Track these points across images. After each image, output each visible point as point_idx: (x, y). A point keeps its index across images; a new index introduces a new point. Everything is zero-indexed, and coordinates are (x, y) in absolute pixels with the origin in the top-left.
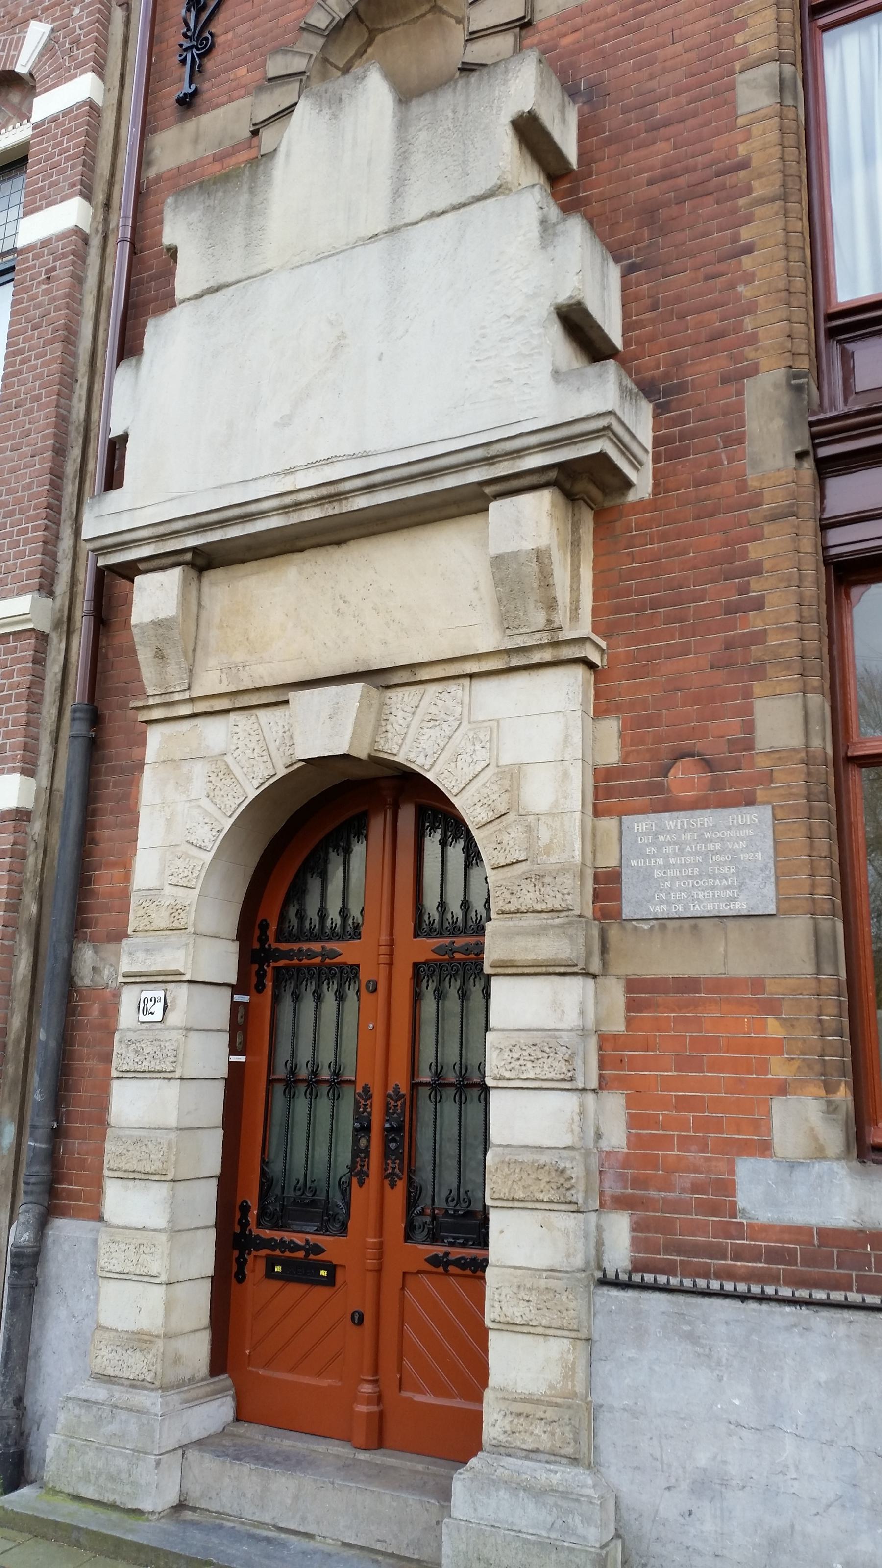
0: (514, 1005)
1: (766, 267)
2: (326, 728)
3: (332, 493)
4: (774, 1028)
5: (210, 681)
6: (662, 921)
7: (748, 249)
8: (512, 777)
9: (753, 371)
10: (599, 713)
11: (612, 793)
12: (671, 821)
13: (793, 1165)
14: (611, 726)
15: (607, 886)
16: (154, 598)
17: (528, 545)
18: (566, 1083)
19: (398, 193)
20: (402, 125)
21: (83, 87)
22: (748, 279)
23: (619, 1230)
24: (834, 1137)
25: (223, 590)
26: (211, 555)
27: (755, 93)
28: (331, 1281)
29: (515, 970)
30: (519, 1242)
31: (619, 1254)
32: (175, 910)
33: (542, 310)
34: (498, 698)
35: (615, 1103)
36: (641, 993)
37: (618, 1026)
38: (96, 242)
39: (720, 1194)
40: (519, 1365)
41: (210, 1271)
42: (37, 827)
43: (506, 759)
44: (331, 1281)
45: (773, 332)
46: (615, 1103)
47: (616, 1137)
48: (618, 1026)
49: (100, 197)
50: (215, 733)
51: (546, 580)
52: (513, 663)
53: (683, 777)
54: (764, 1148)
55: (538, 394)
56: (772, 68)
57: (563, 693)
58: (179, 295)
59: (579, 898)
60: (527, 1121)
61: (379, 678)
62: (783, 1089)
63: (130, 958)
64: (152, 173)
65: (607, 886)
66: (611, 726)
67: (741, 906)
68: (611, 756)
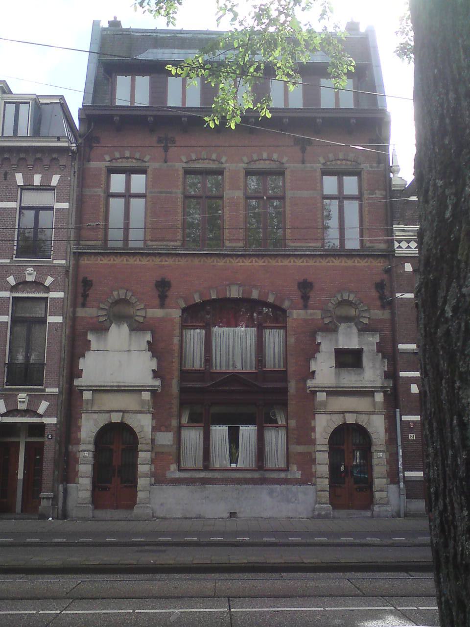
0: (142, 455)
1: (176, 365)
2: (116, 418)
3: (119, 386)
4: (171, 457)
5: (95, 408)
6: (160, 445)
7: (174, 362)
8: (142, 427)
9: (174, 379)
10: (152, 419)
11: (154, 429)
12: (161, 433)
13: (172, 472)
14: (154, 421)
15: (153, 441)
16: (87, 395)
17: (147, 399)
18: (148, 464)
19: (130, 345)
20: (130, 335)
21: (61, 295)
22: (174, 366)
23: (153, 479)
24: (177, 468)
25: (98, 396)
26: (98, 390)
27: (176, 340)
28: (109, 490)
29: (142, 451)
30: (142, 482)
31: (153, 482)
32: (89, 441)
33: (151, 370)
34: (139, 416)
35: (153, 466)
36: (157, 453)
37: (154, 457)
38: (64, 324)
39: (164, 475)
40: (141, 495)
41: (91, 490)
42: (58, 426)
43: (141, 424)
44: (109, 490)
45: (176, 374)
46: (153, 466)
47: (153, 470)
48: (154, 457)
49: (65, 316)
50: (95, 416)
51: (149, 403)
52: (141, 412)
53: (163, 428)
54: (170, 470)
55: (149, 380)
56: (178, 338)
57: (149, 417)
58: (92, 349)
59: (150, 441)
60: (143, 468)
61: (124, 412)
62: (172, 464)
63: (82, 447)
64: (77, 315)
65: (153, 441)
66: (154, 421)
67: (169, 444)
68: (154, 425)
